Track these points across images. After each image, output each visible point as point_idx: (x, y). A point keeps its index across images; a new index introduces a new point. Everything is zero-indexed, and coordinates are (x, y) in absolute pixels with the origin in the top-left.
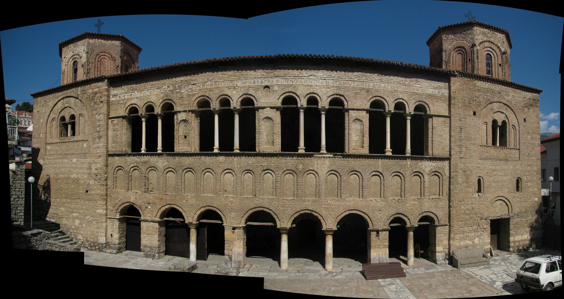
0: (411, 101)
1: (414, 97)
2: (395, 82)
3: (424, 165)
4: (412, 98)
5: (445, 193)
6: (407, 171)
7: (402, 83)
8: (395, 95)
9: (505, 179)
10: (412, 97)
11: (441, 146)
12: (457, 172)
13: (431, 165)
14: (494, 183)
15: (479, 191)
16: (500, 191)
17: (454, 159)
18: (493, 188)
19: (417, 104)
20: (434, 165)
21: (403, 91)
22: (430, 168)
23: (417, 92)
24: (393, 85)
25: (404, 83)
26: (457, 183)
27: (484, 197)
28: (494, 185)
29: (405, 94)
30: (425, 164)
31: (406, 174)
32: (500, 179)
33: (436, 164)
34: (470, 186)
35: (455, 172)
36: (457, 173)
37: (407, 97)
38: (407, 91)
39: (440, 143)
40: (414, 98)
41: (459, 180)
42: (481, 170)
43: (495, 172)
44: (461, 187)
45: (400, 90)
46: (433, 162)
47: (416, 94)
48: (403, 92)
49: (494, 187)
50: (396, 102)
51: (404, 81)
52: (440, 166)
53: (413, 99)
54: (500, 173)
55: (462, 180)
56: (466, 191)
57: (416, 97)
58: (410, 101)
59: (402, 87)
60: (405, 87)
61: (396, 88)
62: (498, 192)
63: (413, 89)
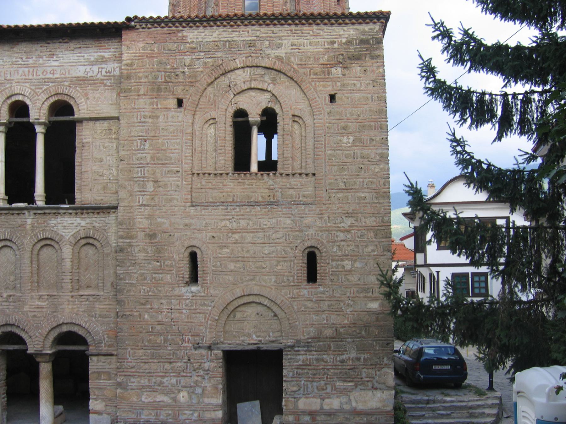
0: (38, 96)
1: (45, 87)
2: (6, 63)
3: (61, 225)
4: (41, 91)
5: (110, 283)
6: (25, 237)
7: (21, 62)
8: (7, 88)
9: (266, 252)
10: (41, 89)
11: (101, 182)
12: (131, 237)
13: (75, 224)
14: (232, 261)
15: (194, 278)
16: (250, 283)
17: (124, 210)
18: (229, 273)
19: (52, 100)
20: (83, 223)
21: (22, 79)
22: (74, 231)
23: (51, 76)
24: (3, 70)
25: (26, 63)
26: (133, 262)
27: (203, 294)
28: (232, 266)
29: (27, 85)
30: (63, 223)
31: (23, 244)
32: (251, 252)
33: (88, 220)
34: (167, 268)
35: (126, 238)
36: (135, 241)
37: (31, 89)
38: (31, 77)
39: (97, 177)
40: (46, 90)
41: (137, 255)
42: (196, 231)
43: (237, 236)
44: (142, 271)
45: (16, 77)
46: (83, 216)
47: (49, 80)
48: (23, 81)
49: (232, 271)
50: (10, 101)
51: (24, 59)
52: (96, 225)
53: (43, 92)
54: (249, 237)
55: (146, 256)
56: (156, 280)
57: (50, 87)
58: (36, 97)
59: (21, 71)
60: (27, 70)
61: (9, 75)
62: (245, 283)
63: (43, 73)
